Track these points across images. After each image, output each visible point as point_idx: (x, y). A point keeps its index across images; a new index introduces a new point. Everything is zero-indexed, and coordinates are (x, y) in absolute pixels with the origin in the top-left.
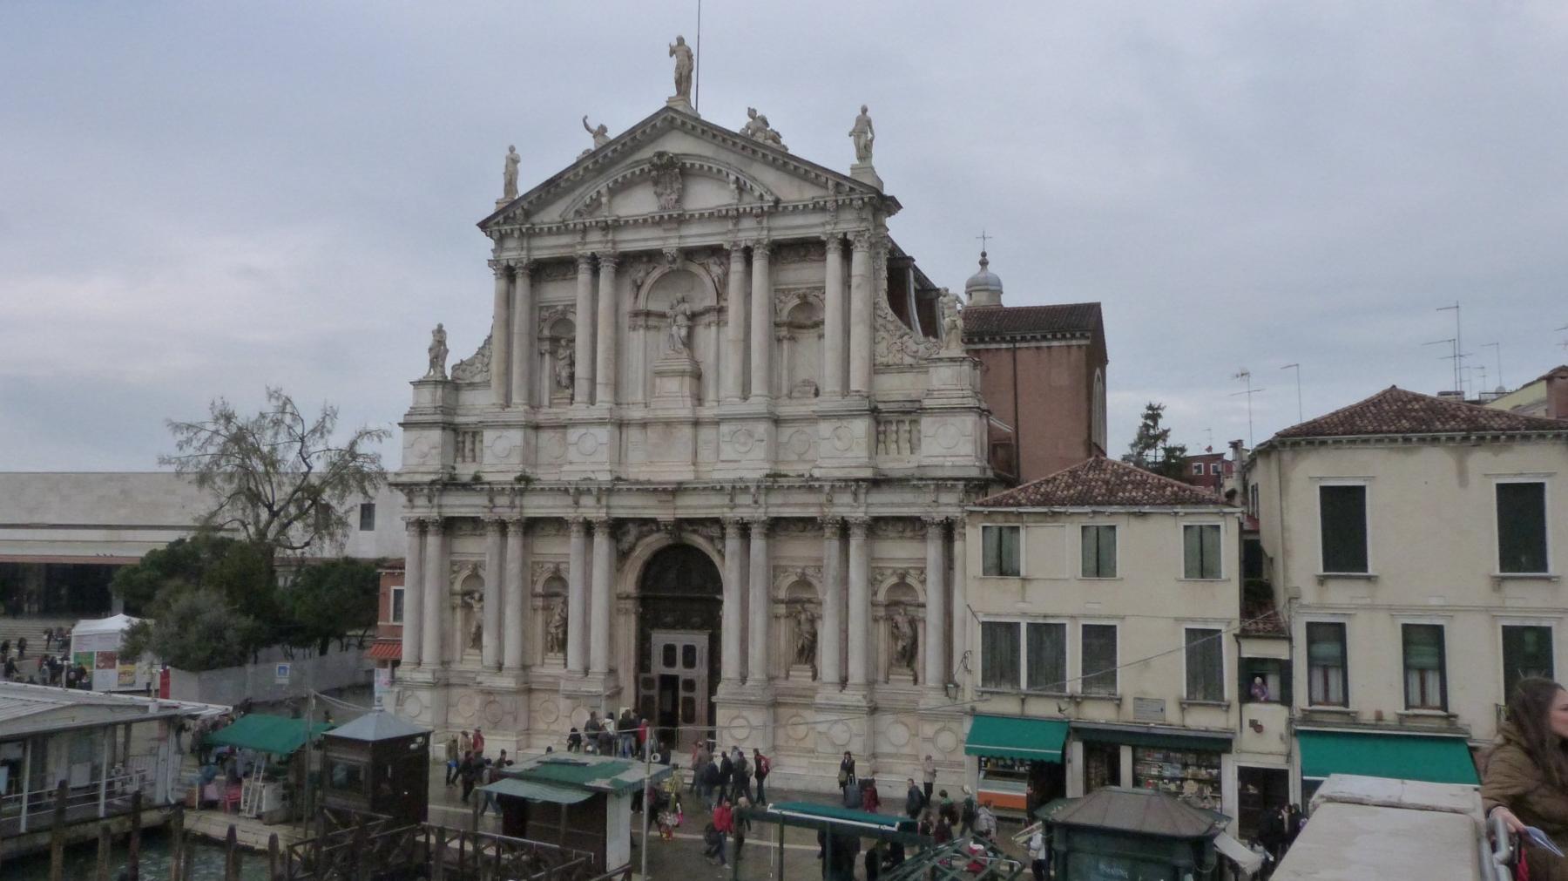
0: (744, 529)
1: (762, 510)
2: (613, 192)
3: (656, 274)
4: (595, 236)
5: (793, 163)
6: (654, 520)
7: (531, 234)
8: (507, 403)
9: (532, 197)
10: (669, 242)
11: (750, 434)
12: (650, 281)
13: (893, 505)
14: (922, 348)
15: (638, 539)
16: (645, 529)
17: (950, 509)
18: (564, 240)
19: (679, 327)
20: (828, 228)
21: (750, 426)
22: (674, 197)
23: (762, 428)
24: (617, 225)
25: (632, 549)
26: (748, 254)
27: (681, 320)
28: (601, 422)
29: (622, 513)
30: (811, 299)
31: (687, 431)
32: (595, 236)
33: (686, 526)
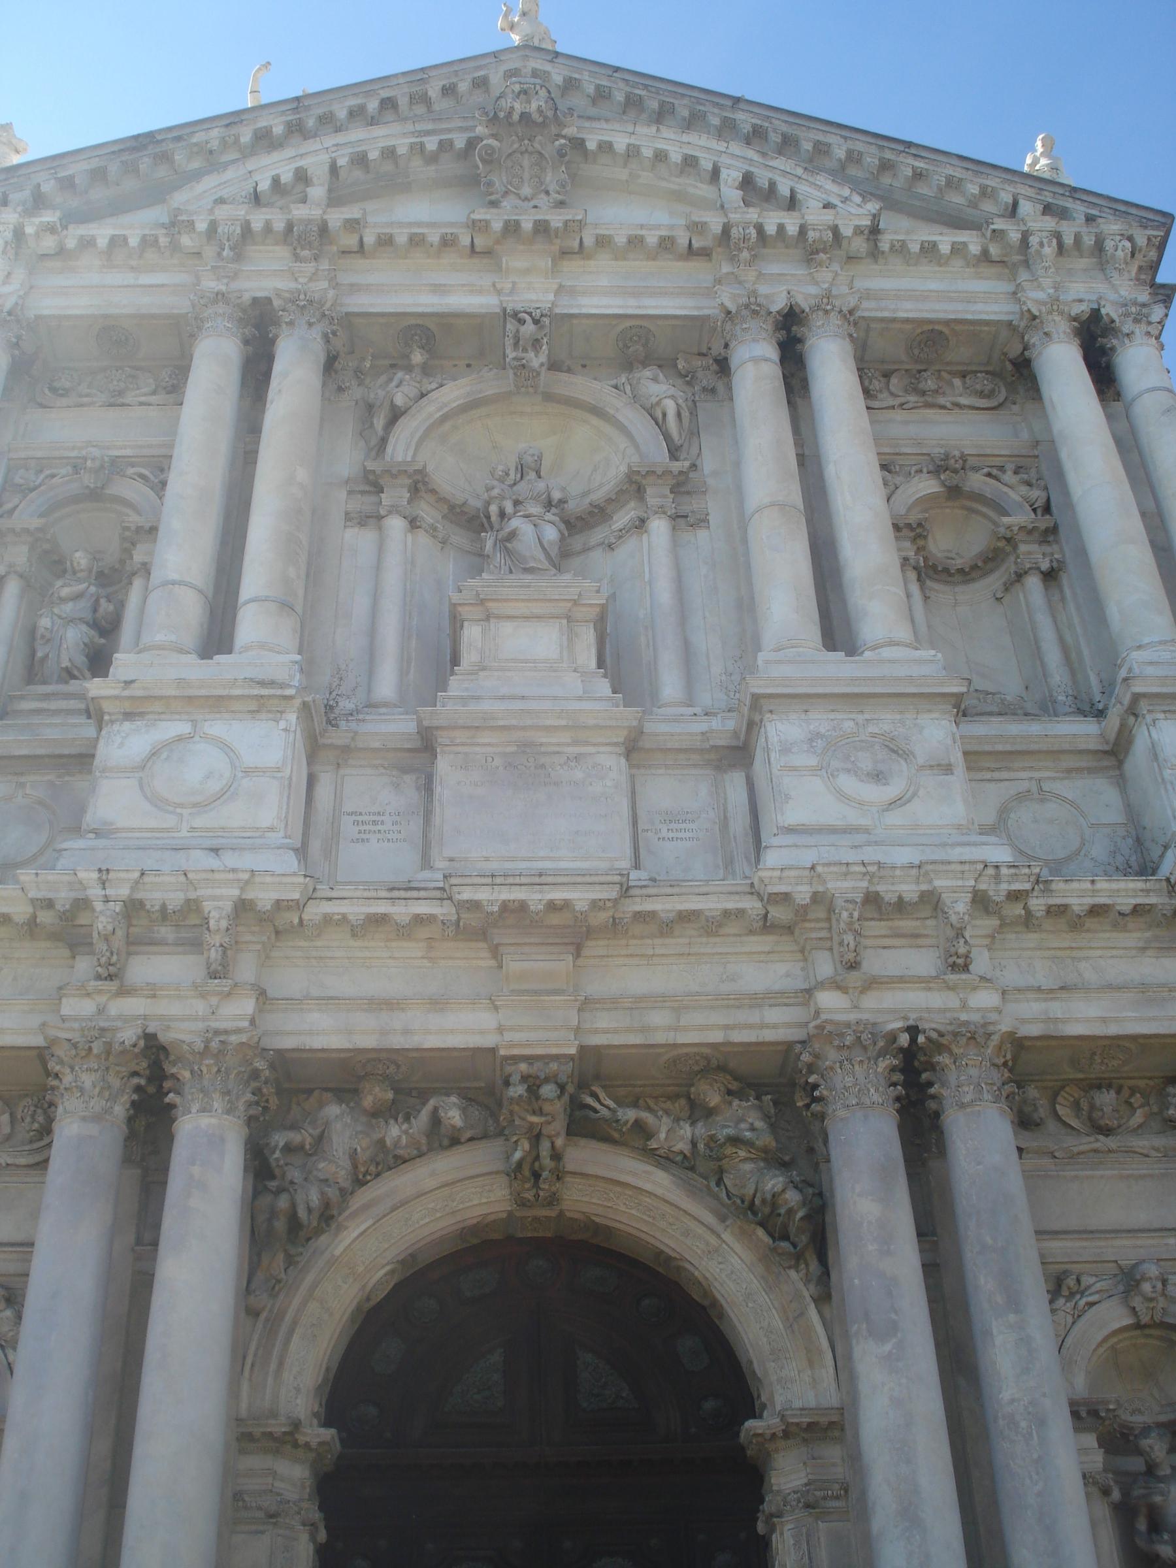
0: (915, 1076)
3: (452, 393)
5: (907, 165)
9: (77, 169)
11: (897, 750)
12: (430, 409)
15: (360, 1182)
16: (394, 1131)
21: (886, 721)
23: (935, 733)
25: (327, 1217)
28: (262, 700)
29: (320, 1031)
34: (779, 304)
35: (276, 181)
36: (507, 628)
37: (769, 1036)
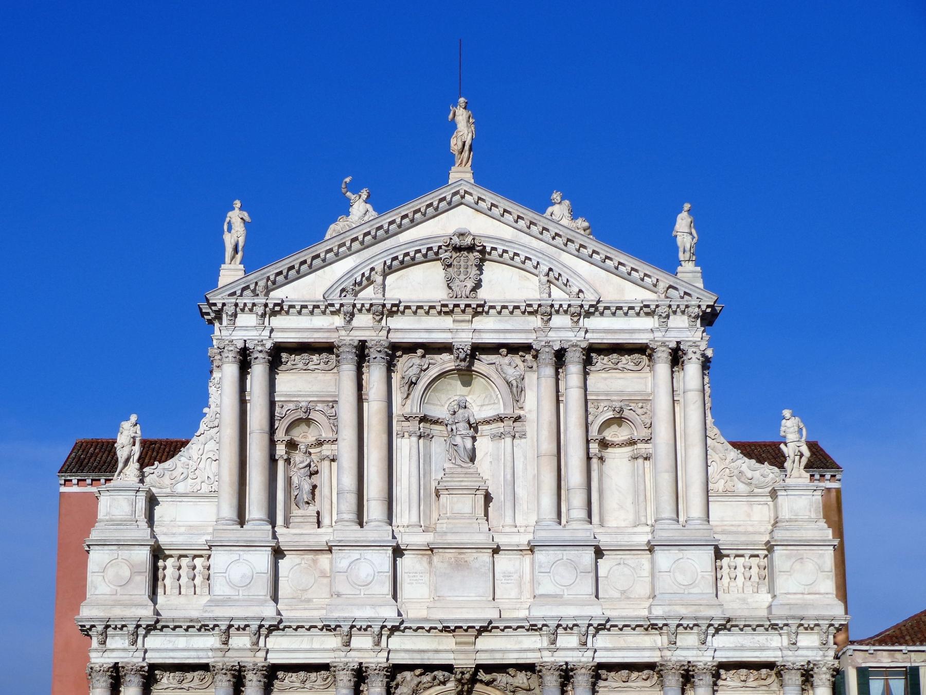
1: (590, 653)
2: (388, 270)
4: (363, 320)
6: (449, 668)
7: (279, 309)
8: (241, 519)
10: (464, 338)
13: (742, 648)
14: (757, 474)
17: (809, 653)
18: (320, 321)
19: (463, 437)
20: (658, 335)
21: (571, 553)
22: (470, 284)
24: (395, 310)
26: (560, 357)
27: (462, 427)
30: (626, 413)
31: (486, 557)
32: (363, 320)
33: (482, 675)
34: (556, 348)
35: (363, 275)
36: (455, 498)
37: (528, 661)
